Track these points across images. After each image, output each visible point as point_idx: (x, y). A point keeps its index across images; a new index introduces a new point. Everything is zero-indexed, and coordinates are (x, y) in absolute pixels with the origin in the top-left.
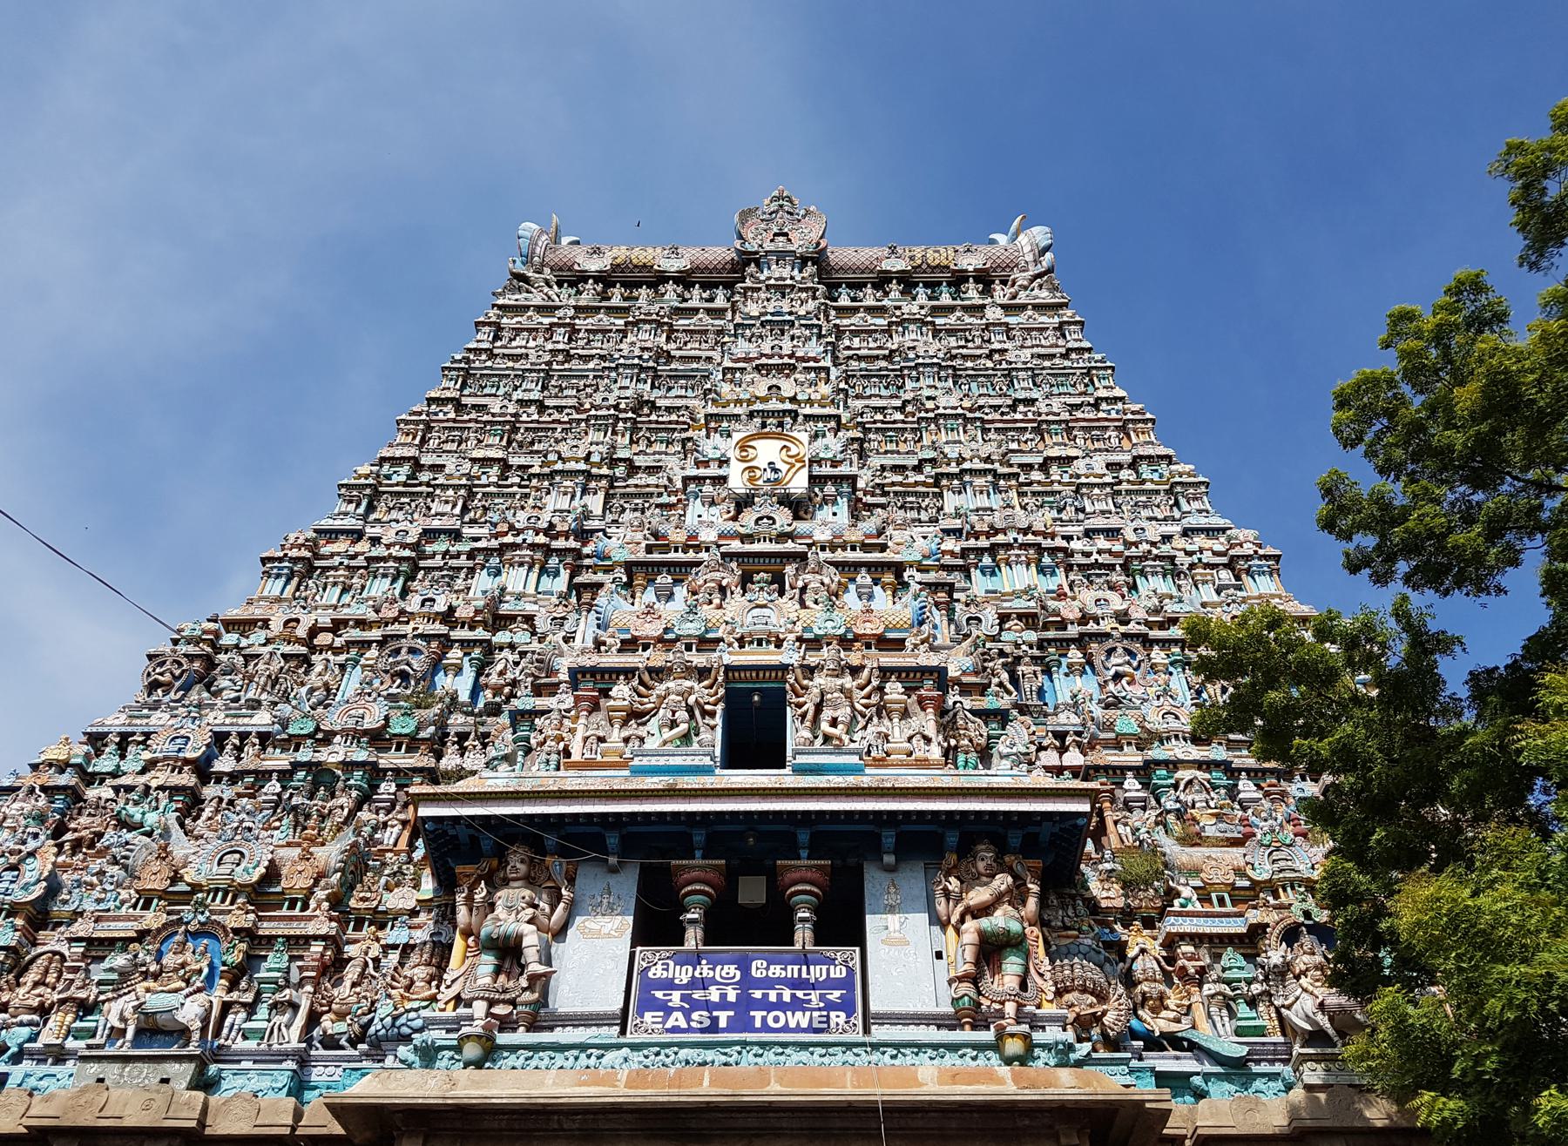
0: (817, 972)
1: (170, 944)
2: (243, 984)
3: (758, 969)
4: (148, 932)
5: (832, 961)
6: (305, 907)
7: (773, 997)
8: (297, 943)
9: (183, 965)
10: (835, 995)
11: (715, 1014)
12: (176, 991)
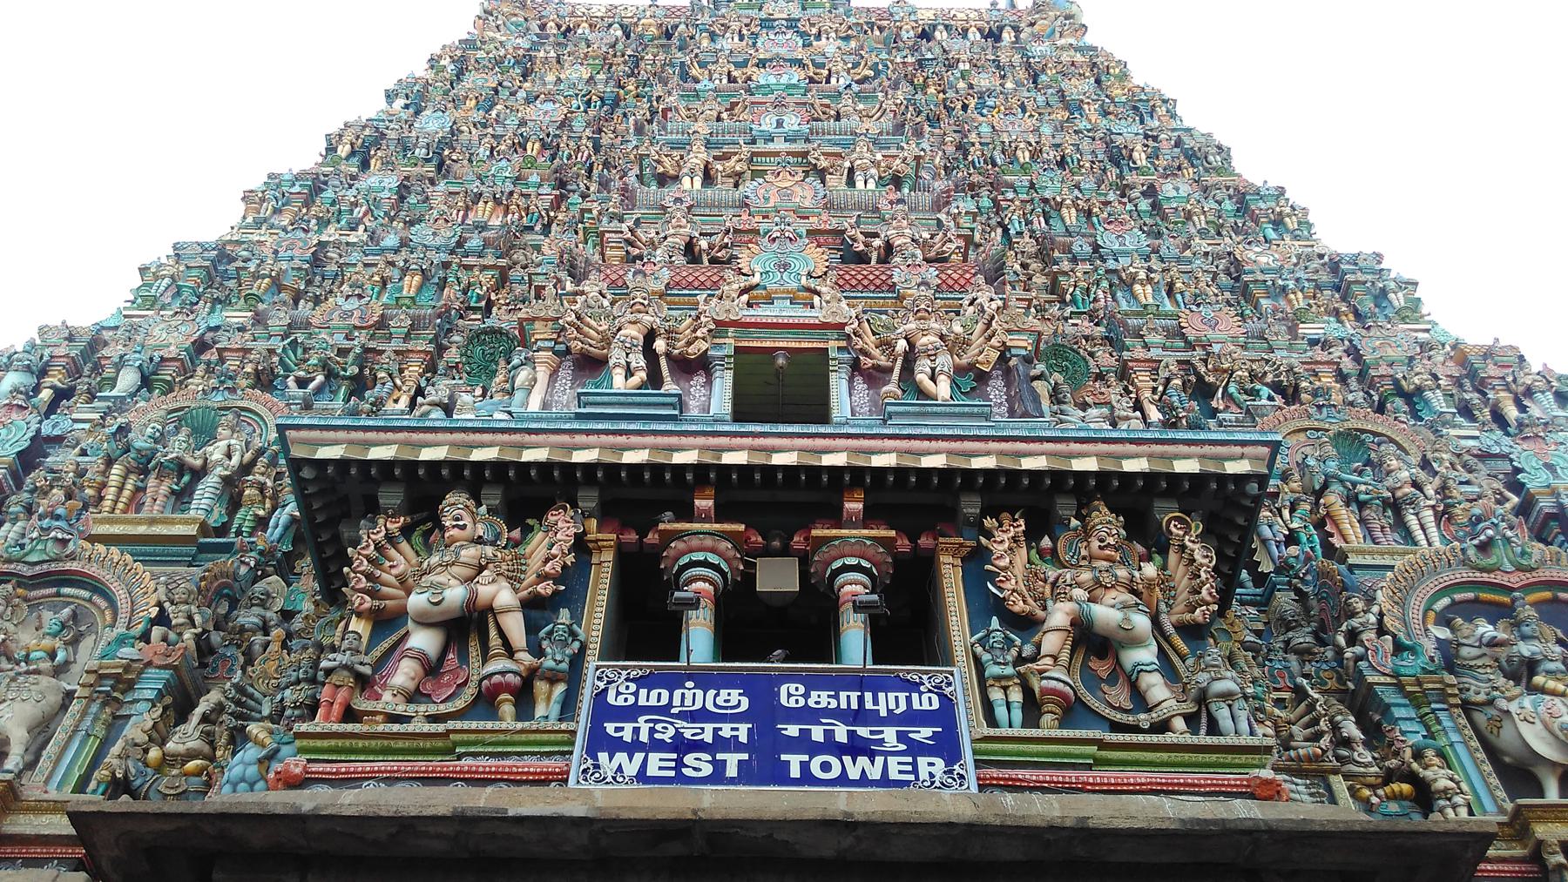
0: (889, 702)
3: (790, 695)
5: (914, 687)
7: (817, 734)
10: (924, 733)
11: (719, 756)
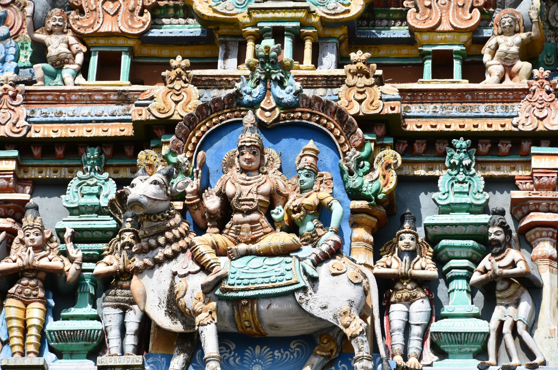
1: (225, 148)
2: (406, 240)
4: (168, 125)
6: (475, 70)
8: (494, 151)
9: (274, 197)
12: (285, 251)
